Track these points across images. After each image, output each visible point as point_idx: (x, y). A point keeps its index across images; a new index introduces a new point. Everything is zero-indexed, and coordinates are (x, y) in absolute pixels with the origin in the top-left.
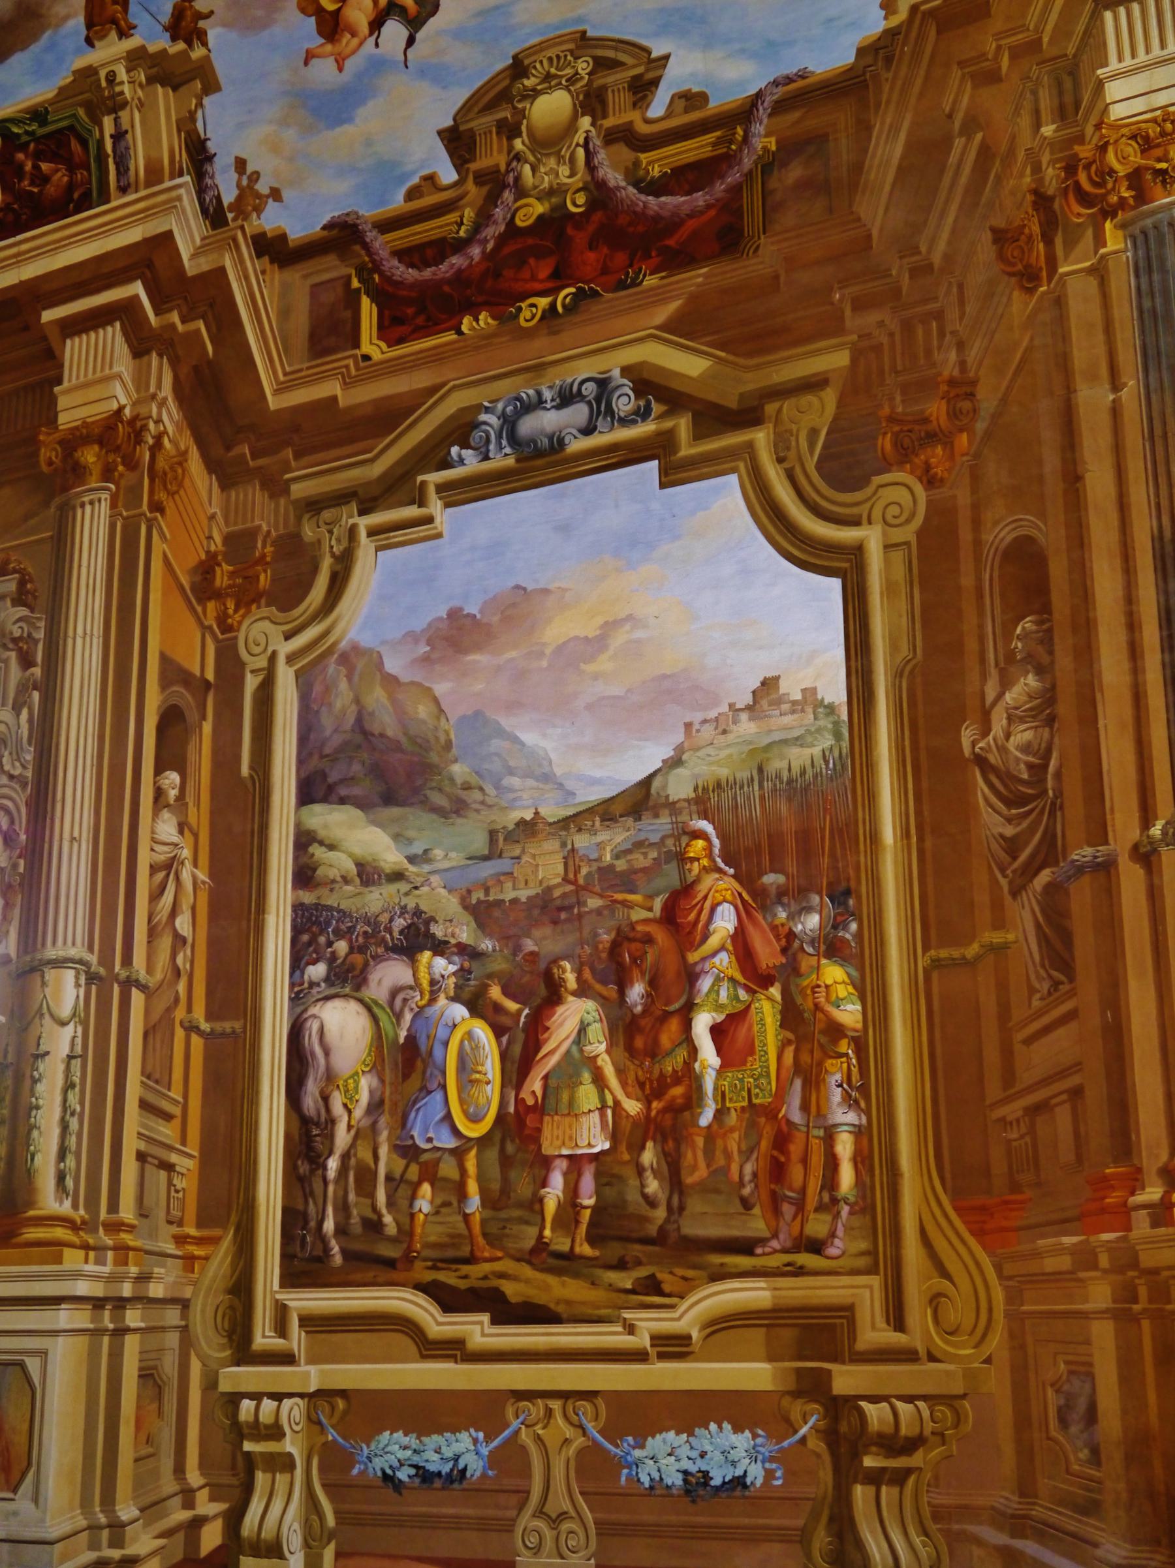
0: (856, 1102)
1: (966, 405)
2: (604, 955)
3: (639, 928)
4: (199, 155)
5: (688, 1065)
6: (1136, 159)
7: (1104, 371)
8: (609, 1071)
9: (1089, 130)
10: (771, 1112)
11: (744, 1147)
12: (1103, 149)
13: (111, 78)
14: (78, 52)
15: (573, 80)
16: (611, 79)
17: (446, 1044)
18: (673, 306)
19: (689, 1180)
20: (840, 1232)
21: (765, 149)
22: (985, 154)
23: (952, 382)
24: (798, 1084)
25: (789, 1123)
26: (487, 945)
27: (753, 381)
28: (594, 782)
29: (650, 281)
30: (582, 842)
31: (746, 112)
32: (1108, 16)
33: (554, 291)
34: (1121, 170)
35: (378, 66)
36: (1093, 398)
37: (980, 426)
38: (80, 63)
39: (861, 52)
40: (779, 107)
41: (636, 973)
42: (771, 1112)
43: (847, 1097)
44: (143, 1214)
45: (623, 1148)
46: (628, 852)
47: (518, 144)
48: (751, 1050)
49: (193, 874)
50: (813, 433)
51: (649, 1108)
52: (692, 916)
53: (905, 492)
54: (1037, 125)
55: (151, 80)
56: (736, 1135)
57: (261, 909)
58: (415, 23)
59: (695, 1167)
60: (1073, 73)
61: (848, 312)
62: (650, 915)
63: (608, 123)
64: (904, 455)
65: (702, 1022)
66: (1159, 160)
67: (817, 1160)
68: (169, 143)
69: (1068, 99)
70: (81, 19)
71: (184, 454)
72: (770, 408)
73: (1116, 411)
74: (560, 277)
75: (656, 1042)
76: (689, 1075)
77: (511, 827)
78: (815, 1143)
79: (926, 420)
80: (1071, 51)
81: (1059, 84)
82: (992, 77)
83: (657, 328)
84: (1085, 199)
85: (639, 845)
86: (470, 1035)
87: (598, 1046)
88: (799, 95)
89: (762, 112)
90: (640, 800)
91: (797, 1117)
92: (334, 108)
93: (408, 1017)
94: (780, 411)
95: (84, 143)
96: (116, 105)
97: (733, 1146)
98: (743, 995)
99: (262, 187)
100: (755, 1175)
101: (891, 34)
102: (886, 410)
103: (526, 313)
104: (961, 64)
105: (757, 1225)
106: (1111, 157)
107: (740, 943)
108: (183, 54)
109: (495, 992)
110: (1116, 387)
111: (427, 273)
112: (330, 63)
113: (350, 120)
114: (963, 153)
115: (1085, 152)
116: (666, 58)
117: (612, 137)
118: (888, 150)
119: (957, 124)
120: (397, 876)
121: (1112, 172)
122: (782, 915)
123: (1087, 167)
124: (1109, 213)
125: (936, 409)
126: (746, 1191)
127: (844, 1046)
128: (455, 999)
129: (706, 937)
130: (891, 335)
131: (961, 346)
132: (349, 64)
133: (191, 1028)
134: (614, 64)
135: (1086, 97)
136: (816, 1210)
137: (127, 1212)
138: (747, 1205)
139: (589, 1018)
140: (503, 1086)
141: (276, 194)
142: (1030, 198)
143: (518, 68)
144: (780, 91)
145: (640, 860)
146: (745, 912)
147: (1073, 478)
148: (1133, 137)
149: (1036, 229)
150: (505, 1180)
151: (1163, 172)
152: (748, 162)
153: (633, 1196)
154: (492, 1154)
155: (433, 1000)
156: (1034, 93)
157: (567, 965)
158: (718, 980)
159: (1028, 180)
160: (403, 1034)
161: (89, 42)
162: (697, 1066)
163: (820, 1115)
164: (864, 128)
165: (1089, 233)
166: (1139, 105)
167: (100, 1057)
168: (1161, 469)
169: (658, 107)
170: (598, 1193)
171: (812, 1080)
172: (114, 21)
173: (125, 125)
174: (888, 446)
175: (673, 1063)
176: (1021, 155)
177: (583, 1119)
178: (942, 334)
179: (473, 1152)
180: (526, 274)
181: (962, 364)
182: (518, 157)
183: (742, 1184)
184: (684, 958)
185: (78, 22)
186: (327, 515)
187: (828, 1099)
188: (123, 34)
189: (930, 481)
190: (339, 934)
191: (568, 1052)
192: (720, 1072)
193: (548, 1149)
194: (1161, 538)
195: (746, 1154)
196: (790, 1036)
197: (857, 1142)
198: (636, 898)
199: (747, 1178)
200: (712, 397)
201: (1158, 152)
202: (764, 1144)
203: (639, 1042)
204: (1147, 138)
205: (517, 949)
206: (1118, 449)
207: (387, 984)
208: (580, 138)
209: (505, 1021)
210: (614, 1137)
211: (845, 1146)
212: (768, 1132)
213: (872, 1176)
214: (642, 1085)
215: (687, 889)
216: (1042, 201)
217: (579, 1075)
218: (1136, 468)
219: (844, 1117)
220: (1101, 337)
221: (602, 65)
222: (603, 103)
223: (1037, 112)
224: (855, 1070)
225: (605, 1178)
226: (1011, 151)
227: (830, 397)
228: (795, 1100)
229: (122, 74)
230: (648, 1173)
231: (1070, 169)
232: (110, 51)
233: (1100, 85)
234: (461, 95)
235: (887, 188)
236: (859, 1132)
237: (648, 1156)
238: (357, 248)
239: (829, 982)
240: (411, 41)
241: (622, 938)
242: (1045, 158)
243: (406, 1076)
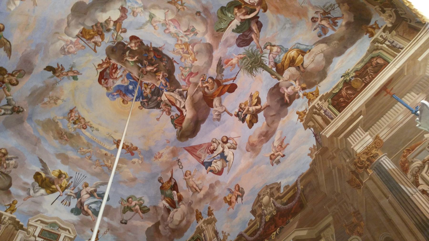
1: (359, 216)
4: (216, 233)
6: (366, 157)
7: (383, 196)
9: (355, 157)
12: (359, 158)
13: (202, 227)
14: (196, 225)
15: (267, 193)
16: (273, 190)
18: (297, 223)
21: (302, 188)
22: (339, 170)
23: (354, 213)
27: (316, 231)
29: (291, 220)
31: (296, 184)
32: (348, 139)
33: (276, 230)
34: (365, 160)
35: (238, 206)
36: (384, 202)
37: (364, 219)
38: (197, 226)
39: (310, 165)
40: (301, 181)
47: (263, 208)
50: (332, 235)
53: (356, 240)
54: (345, 161)
55: (207, 224)
58: (242, 197)
60: (347, 150)
61: (328, 209)
63: (275, 197)
64: (352, 232)
66: (371, 155)
68: (212, 233)
69: (348, 154)
70: (196, 219)
72: (322, 235)
73: (390, 202)
74: (276, 227)
79: (353, 223)
80: (345, 147)
81: (345, 152)
82: (334, 158)
83: (296, 228)
84: (361, 168)
88: (303, 177)
89: (299, 183)
92: (234, 216)
94: (324, 234)
95: (200, 239)
96: (203, 231)
99: (226, 234)
101: (314, 161)
102: (344, 224)
103: (273, 237)
104: (328, 158)
106: (361, 159)
108: (211, 218)
110: (387, 198)
111: (255, 237)
112: (232, 209)
113: (237, 217)
114: (335, 172)
115: (356, 160)
116: (280, 182)
117: (276, 199)
118: (322, 178)
119: (331, 167)
121: (363, 161)
123: (358, 162)
124: (366, 168)
125: (354, 219)
130: (338, 209)
131: (352, 205)
132: (234, 208)
134: (273, 188)
135: (351, 152)
141: (229, 234)
142: (351, 173)
143: (259, 196)
144: (300, 179)
147: (389, 220)
148: (364, 154)
149: (355, 177)
151: (373, 156)
152: (299, 192)
156: (342, 156)
159: (349, 170)
161: (197, 222)
164: (316, 176)
165: (365, 173)
166: (361, 148)
168: (407, 209)
169: (282, 191)
172: (200, 218)
173: (205, 233)
174: (348, 231)
176: (345, 167)
178: (348, 205)
180: (270, 229)
181: (354, 208)
182: (263, 210)
185: (195, 220)
188: (202, 219)
189: (360, 235)
194: (416, 224)
200: (310, 237)
201: (370, 153)
204: (366, 153)
206: (395, 209)
208: (272, 202)
216: (353, 172)
218: (402, 212)
220: (378, 190)
221: (271, 189)
222: (273, 194)
223: (344, 159)
226: (343, 167)
227: (332, 227)
229: (203, 225)
231: (355, 164)
232: (201, 221)
233: (353, 149)
234: (251, 204)
235: (325, 184)
238: (243, 238)
240: (242, 199)
242: (350, 165)
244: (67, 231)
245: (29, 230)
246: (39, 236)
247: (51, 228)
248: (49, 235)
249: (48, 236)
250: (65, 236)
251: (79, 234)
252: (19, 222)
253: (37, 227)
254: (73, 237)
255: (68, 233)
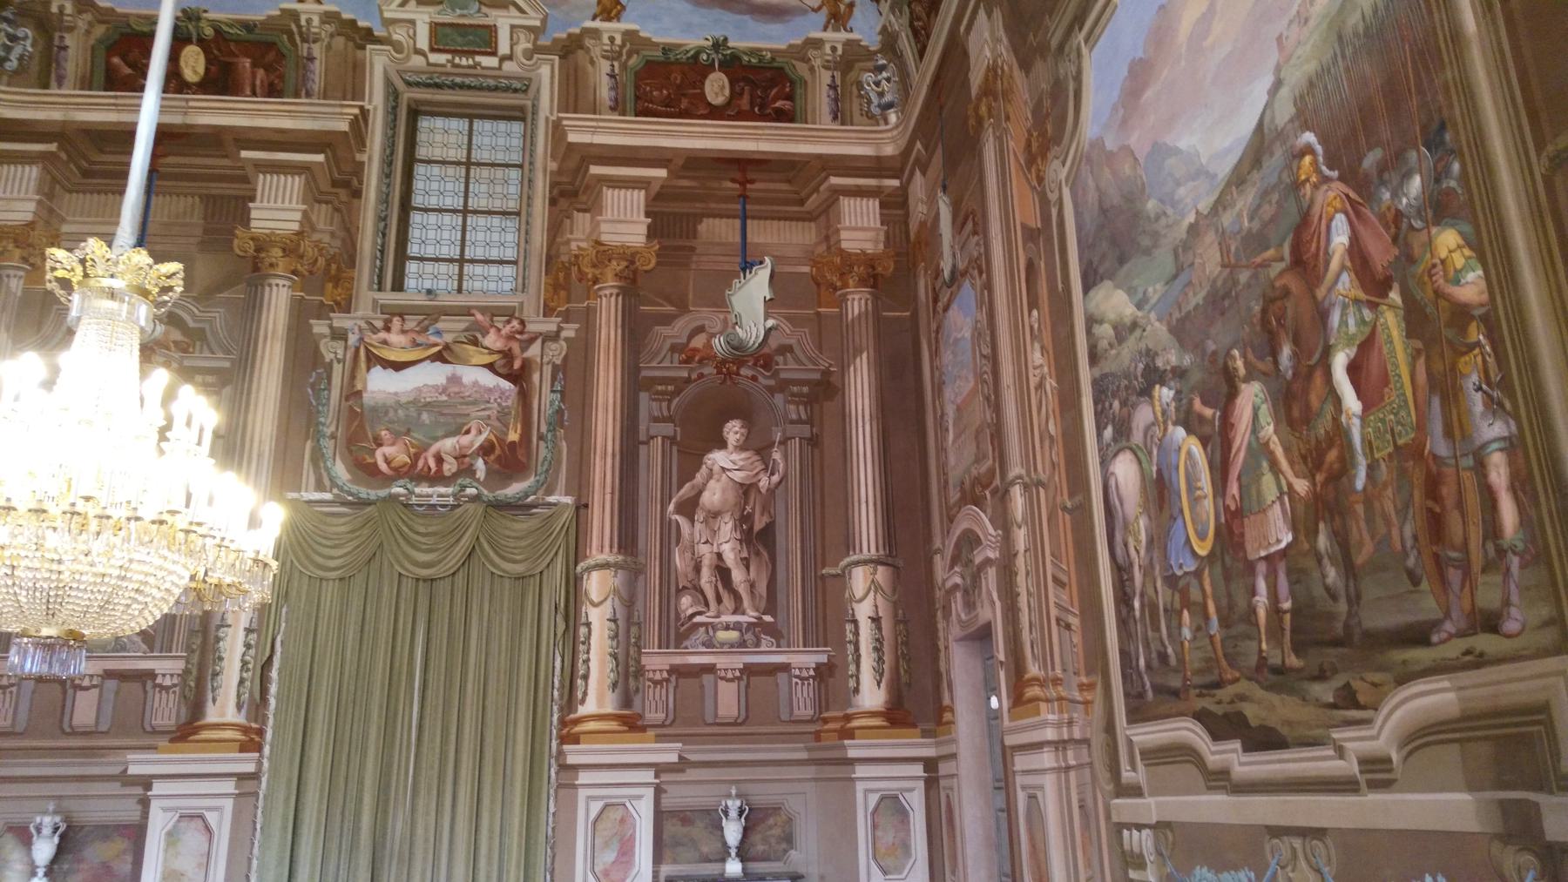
0: (1501, 405)
2: (1258, 328)
3: (1278, 284)
5: (1336, 420)
8: (1279, 452)
10: (1415, 451)
11: (1399, 506)
17: (1177, 468)
19: (1359, 559)
20: (1515, 598)
24: (1436, 402)
25: (1435, 457)
26: (1187, 360)
28: (1228, 151)
30: (1227, 219)
41: (1283, 335)
42: (1415, 451)
43: (1489, 401)
44: (1064, 670)
45: (1302, 538)
46: (1259, 206)
48: (1385, 381)
49: (1050, 383)
51: (1314, 484)
52: (1314, 245)
56: (1389, 492)
57: (1079, 396)
59: (1361, 544)
62: (1282, 265)
65: (1340, 361)
67: (1473, 500)
71: (1011, 68)
75: (1308, 407)
76: (1339, 433)
77: (1184, 236)
78: (1466, 475)
85: (1265, 194)
86: (1189, 454)
87: (1269, 430)
90: (1260, 144)
91: (1443, 449)
93: (1155, 452)
97: (1389, 507)
98: (1367, 314)
100: (1415, 538)
105: (1427, 606)
107: (1356, 251)
109: (1197, 404)
120: (1134, 325)
122: (1387, 195)
126: (1411, 562)
127: (1476, 334)
128: (1175, 424)
129: (1327, 263)
133: (1064, 509)
136: (1484, 571)
137: (1058, 671)
138: (1415, 580)
139: (1258, 401)
140: (1215, 497)
145: (1268, 211)
146: (1355, 214)
150: (1229, 595)
153: (1318, 591)
154: (1218, 569)
155: (1166, 429)
157: (1236, 352)
158: (1345, 307)
160: (1154, 469)
162: (1343, 419)
163: (1466, 437)
167: (1035, 548)
170: (1293, 595)
171: (1446, 388)
175: (1322, 427)
177: (1270, 513)
179: (1207, 572)
183: (1405, 554)
184: (1314, 297)
186: (1067, 49)
187: (1470, 412)
190: (1114, 396)
191: (1249, 444)
192: (1363, 418)
193: (1252, 556)
195: (1402, 512)
196: (1419, 344)
197: (1511, 463)
198: (1271, 253)
199: (1409, 543)
202: (1417, 494)
203: (1296, 413)
205: (1204, 351)
207: (1142, 426)
209: (1207, 430)
210: (1294, 529)
211: (1499, 472)
212: (1418, 476)
213: (1537, 505)
214: (1304, 458)
215: (1305, 218)
217: (1259, 466)
219: (1493, 430)
224: (1491, 360)
225: (1297, 577)
228: (1437, 427)
230: (1326, 561)
236: (1512, 446)
237: (1323, 542)
239: (1443, 254)
241: (1268, 302)
243: (1161, 508)
244: (512, 8)
245: (395, 37)
246: (433, 50)
247: (458, 12)
248: (463, 36)
249: (459, 39)
250: (513, 27)
251: (553, 6)
252: (353, 22)
253: (413, 22)
254: (538, 23)
255: (518, 14)
